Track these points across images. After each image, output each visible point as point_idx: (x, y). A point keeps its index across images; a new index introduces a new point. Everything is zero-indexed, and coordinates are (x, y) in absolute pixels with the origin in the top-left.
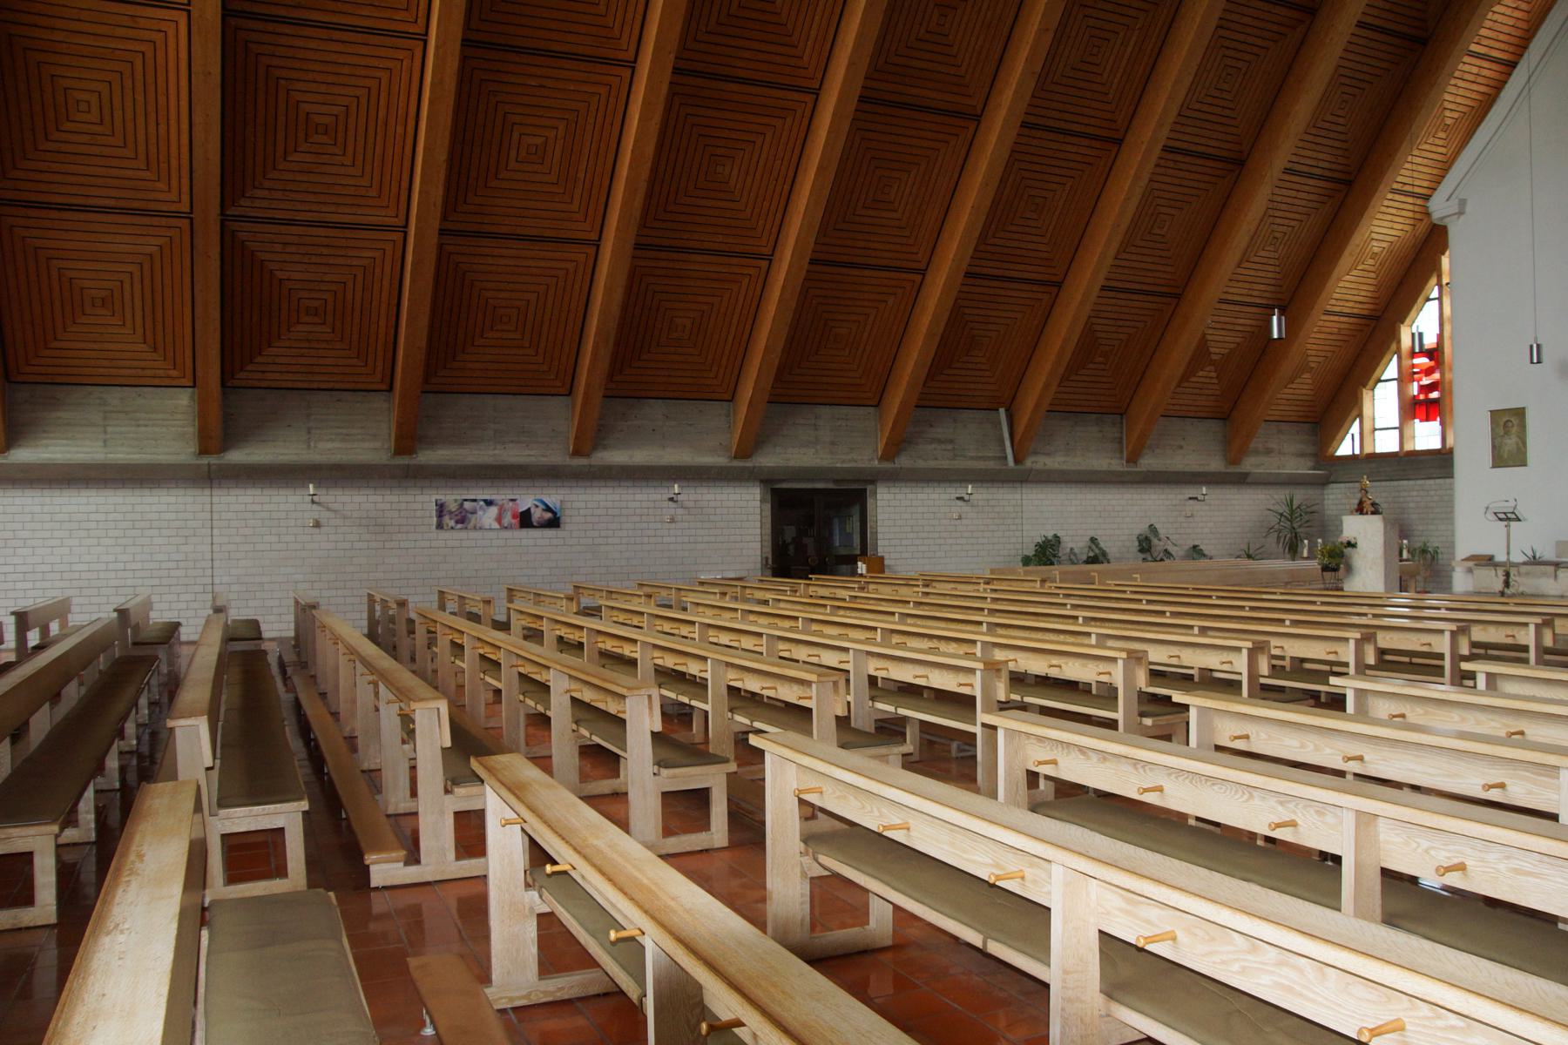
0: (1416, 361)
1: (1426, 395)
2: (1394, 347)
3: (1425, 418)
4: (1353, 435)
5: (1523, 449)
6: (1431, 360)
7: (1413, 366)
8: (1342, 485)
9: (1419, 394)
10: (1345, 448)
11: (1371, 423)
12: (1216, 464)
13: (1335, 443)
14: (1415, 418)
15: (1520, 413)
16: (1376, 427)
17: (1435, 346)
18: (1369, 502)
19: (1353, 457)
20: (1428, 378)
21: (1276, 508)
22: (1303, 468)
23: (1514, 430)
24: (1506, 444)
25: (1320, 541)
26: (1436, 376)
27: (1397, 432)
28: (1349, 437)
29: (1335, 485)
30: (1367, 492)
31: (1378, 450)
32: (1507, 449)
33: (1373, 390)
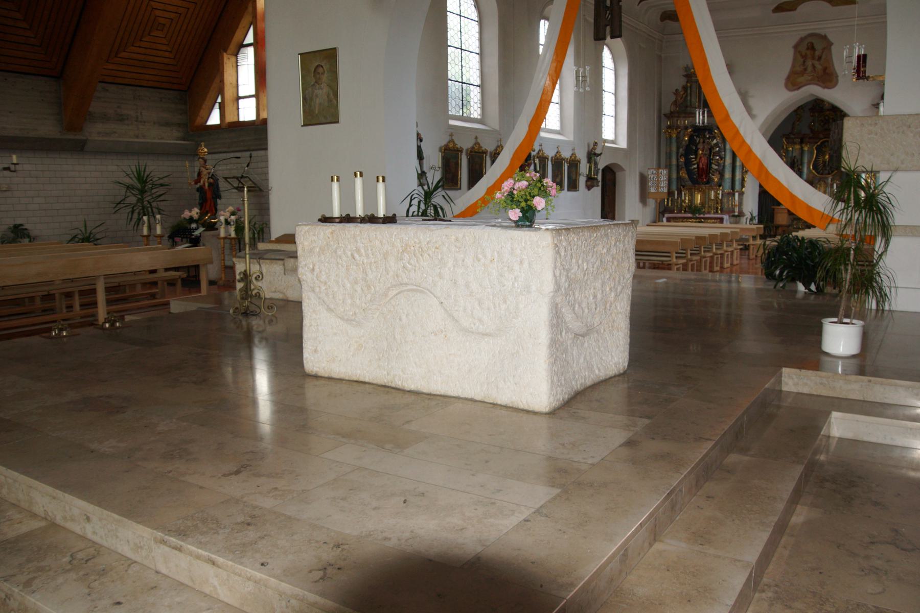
5: (334, 101)
10: (214, 119)
11: (235, 90)
12: (48, 128)
13: (203, 113)
15: (331, 55)
16: (241, 94)
21: (127, 181)
22: (171, 137)
23: (325, 78)
24: (317, 96)
30: (205, 161)
31: (241, 119)
32: (318, 101)
33: (236, 55)
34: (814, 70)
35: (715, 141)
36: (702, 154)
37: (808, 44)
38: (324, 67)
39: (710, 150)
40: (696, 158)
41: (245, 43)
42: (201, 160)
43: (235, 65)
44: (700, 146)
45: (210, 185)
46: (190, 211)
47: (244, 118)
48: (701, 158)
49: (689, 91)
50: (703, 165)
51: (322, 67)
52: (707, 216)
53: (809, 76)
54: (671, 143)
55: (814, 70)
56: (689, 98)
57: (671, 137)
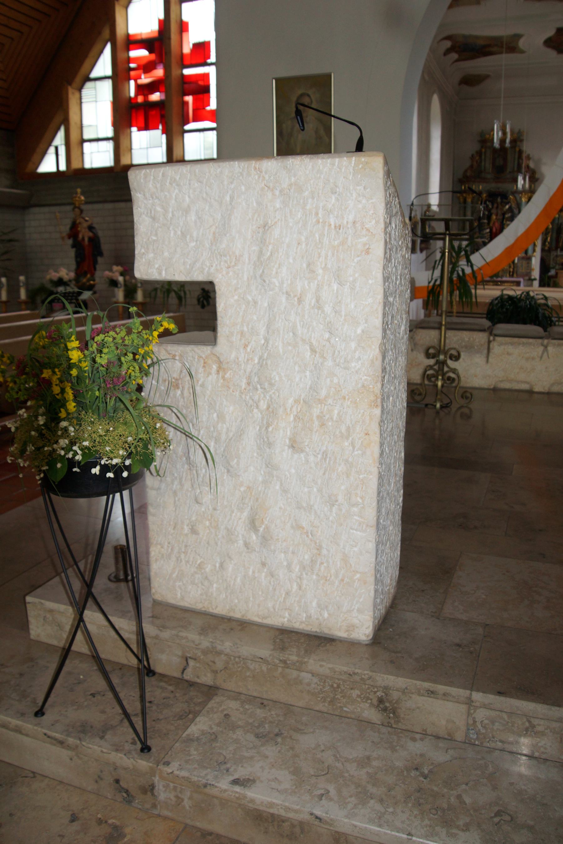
0: (133, 54)
1: (146, 96)
2: (106, 33)
3: (142, 125)
4: (57, 148)
6: (150, 52)
7: (129, 60)
8: (46, 209)
9: (137, 94)
13: (35, 157)
14: (131, 126)
16: (86, 137)
17: (156, 35)
18: (85, 225)
19: (58, 174)
20: (148, 75)
25: (22, 278)
26: (159, 72)
27: (110, 146)
28: (52, 150)
29: (36, 210)
30: (82, 211)
31: (87, 165)
35: (507, 207)
36: (496, 218)
38: (312, 96)
39: (504, 214)
40: (489, 223)
41: (93, 75)
42: (77, 210)
43: (79, 101)
44: (494, 211)
45: (90, 239)
46: (56, 271)
47: (91, 164)
48: (494, 223)
49: (483, 157)
50: (496, 230)
51: (308, 95)
52: (504, 279)
54: (465, 208)
56: (483, 163)
57: (465, 201)
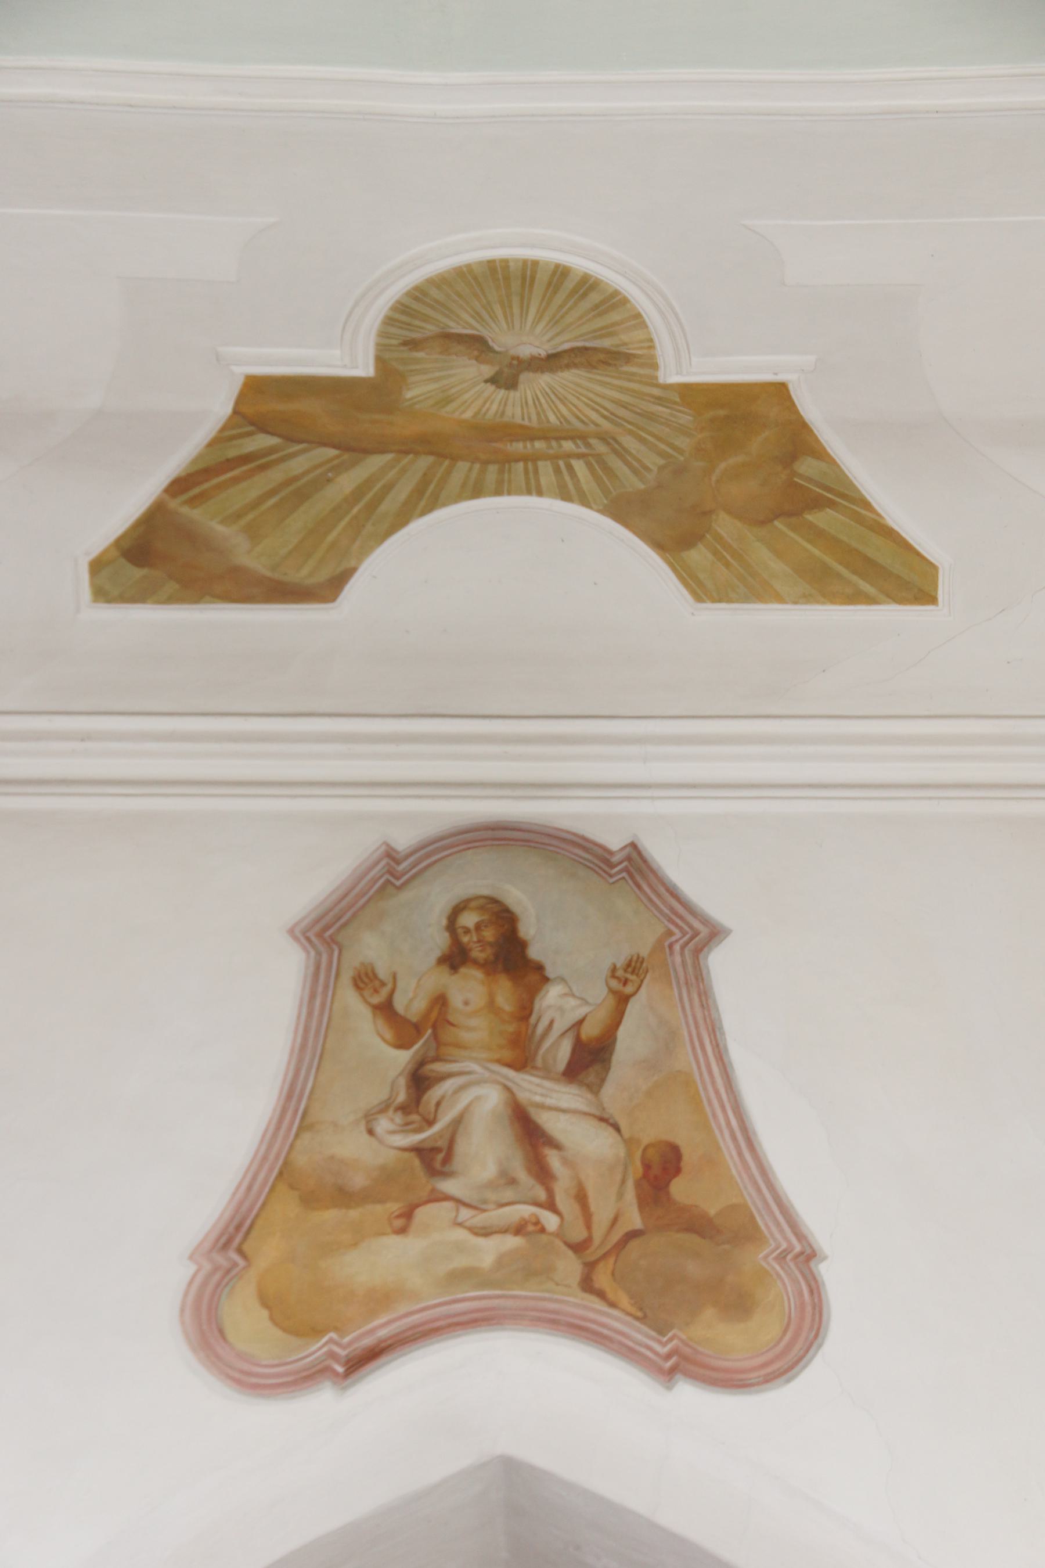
34: (542, 1173)
37: (456, 912)
53: (485, 1232)
55: (542, 1173)
